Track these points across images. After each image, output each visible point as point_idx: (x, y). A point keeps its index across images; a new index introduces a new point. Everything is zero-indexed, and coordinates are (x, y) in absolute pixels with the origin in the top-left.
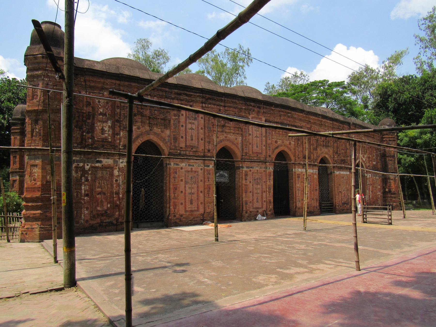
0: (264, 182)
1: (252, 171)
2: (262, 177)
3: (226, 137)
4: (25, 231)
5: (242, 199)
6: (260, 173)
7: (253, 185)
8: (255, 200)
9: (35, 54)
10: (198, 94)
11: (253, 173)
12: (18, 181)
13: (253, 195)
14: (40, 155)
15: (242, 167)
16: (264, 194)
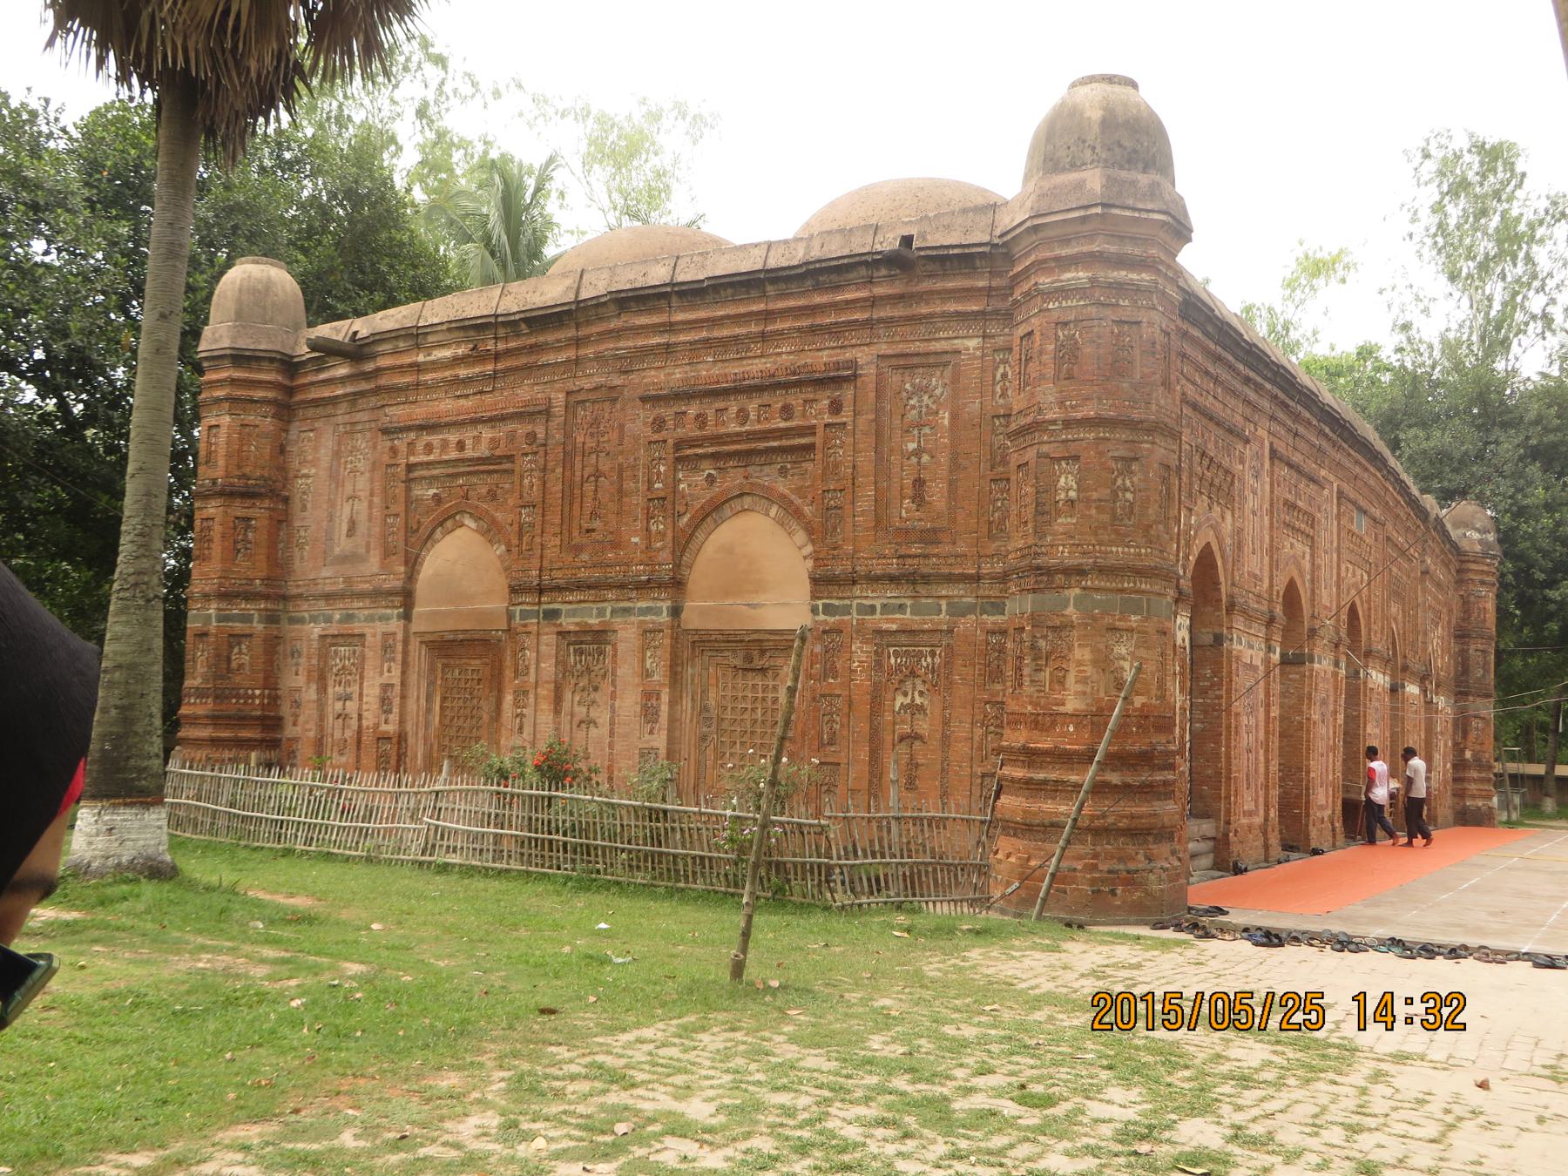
3: (1292, 545)
4: (1103, 881)
5: (1308, 772)
9: (1140, 206)
10: (1268, 386)
12: (257, 642)
14: (1143, 592)
15: (1312, 661)
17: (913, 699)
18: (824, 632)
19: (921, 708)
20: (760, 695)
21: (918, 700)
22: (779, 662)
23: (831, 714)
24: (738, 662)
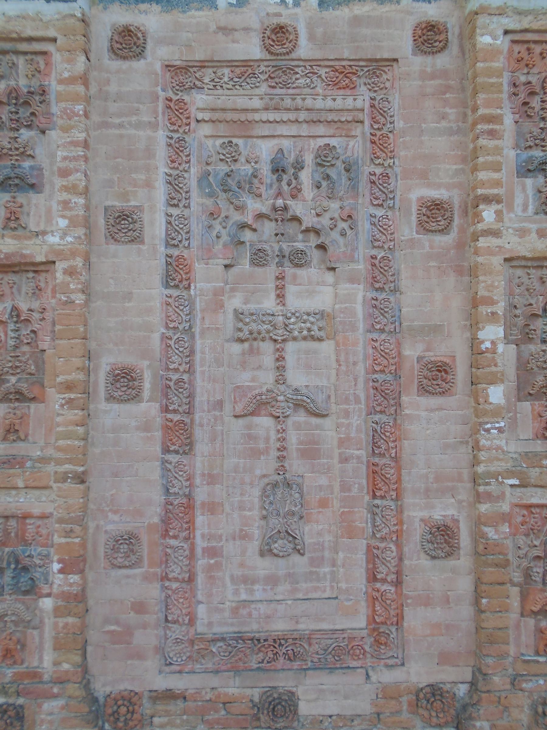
0: (434, 214)
1: (158, 55)
2: (380, 144)
6: (343, 76)
7: (176, 274)
8: (231, 518)
11: (183, 74)
13: (178, 436)
16: (429, 428)
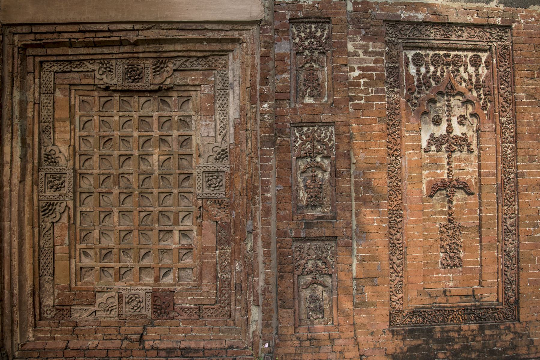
17: (450, 130)
18: (295, 21)
19: (463, 142)
20: (156, 133)
21: (458, 130)
22: (191, 78)
23: (311, 155)
24: (114, 80)
